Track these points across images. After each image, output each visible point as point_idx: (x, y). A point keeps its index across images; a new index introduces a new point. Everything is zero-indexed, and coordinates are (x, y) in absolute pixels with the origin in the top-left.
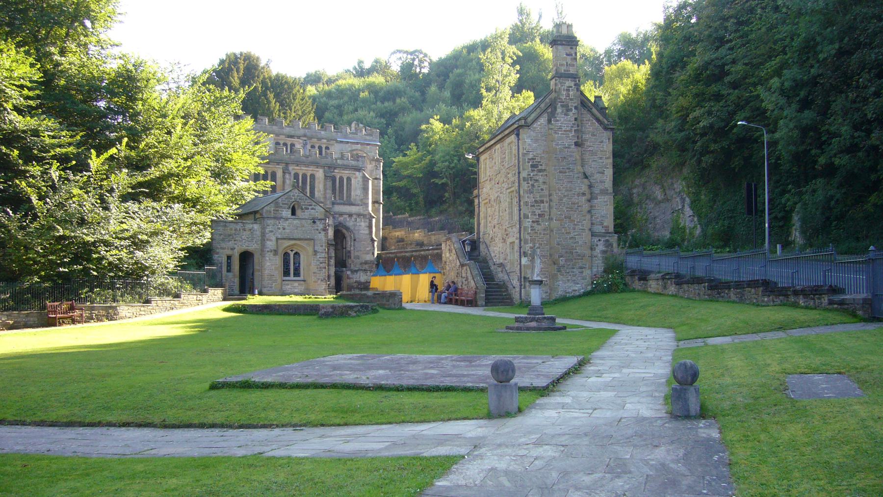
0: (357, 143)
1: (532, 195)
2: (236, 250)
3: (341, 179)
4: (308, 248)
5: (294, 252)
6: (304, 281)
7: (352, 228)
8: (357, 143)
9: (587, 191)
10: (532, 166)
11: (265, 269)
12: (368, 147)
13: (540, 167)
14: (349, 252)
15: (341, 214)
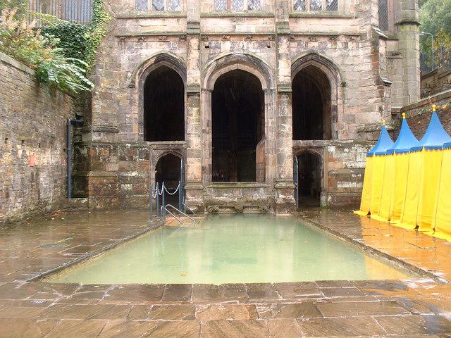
7: (337, 62)
14: (336, 108)
15: (313, 37)
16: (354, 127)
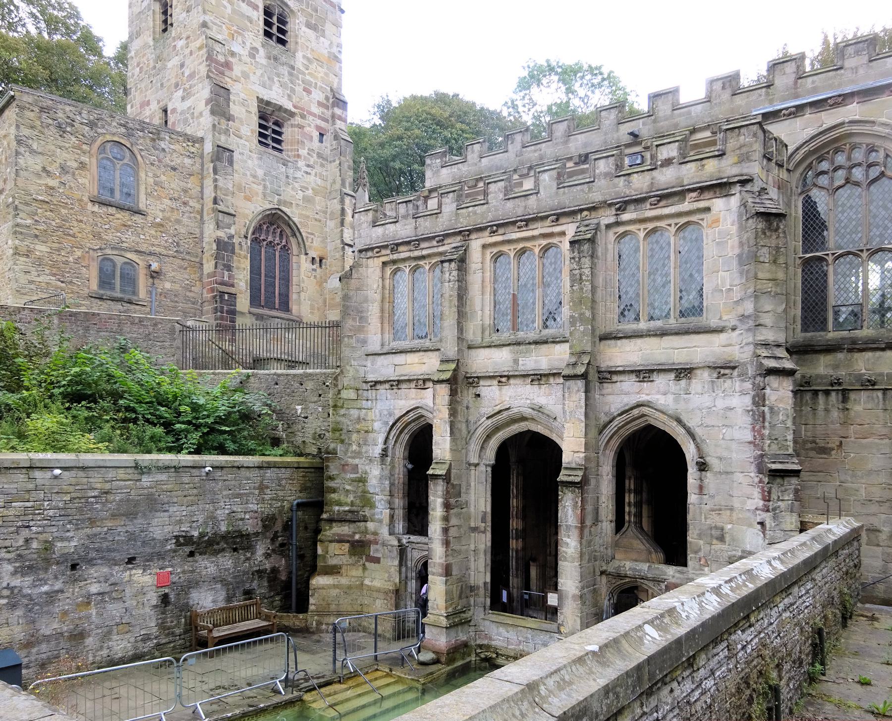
15: (644, 374)
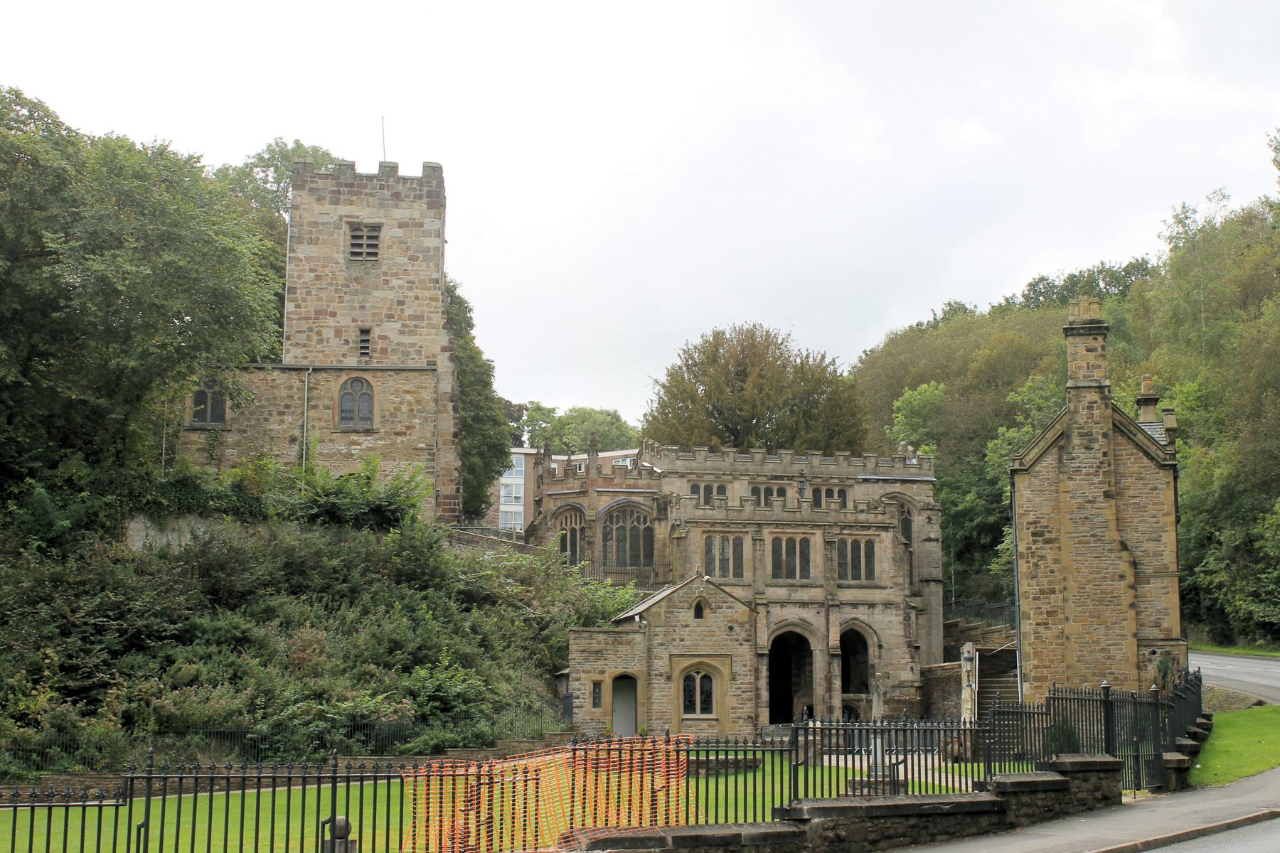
0: (896, 481)
1: (1034, 582)
2: (607, 675)
3: (856, 545)
4: (721, 668)
5: (700, 675)
6: (717, 720)
8: (896, 481)
9: (1129, 572)
10: (1034, 534)
11: (652, 704)
12: (915, 486)
13: (1047, 536)
15: (854, 605)
16: (890, 682)
